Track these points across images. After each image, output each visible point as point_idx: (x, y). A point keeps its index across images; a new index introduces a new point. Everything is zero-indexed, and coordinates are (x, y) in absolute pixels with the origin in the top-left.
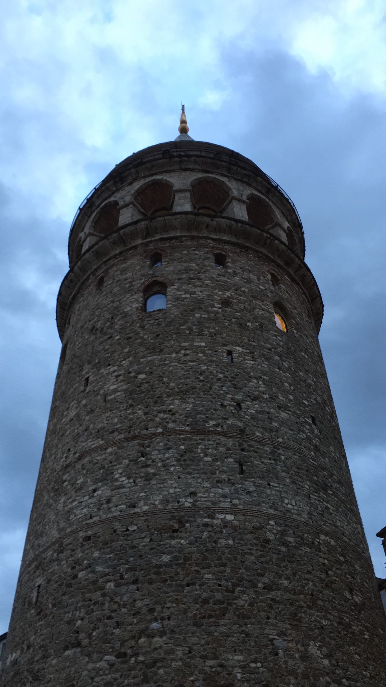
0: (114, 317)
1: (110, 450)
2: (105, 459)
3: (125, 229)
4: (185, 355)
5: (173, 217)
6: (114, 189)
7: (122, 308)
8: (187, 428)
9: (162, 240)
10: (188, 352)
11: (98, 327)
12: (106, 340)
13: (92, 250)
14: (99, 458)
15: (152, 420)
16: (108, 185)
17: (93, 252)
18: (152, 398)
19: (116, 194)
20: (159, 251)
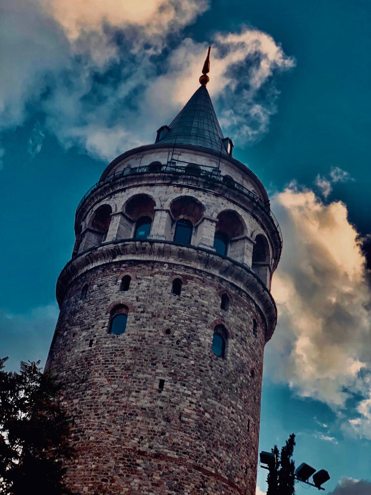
0: (191, 339)
1: (182, 468)
2: (178, 474)
3: (214, 256)
4: (233, 413)
5: (247, 274)
6: (201, 187)
7: (199, 334)
8: (227, 478)
9: (232, 284)
10: (234, 411)
11: (175, 334)
12: (182, 356)
13: (180, 247)
14: (174, 469)
15: (210, 460)
16: (200, 179)
17: (180, 250)
18: (212, 440)
19: (201, 193)
20: (228, 295)
